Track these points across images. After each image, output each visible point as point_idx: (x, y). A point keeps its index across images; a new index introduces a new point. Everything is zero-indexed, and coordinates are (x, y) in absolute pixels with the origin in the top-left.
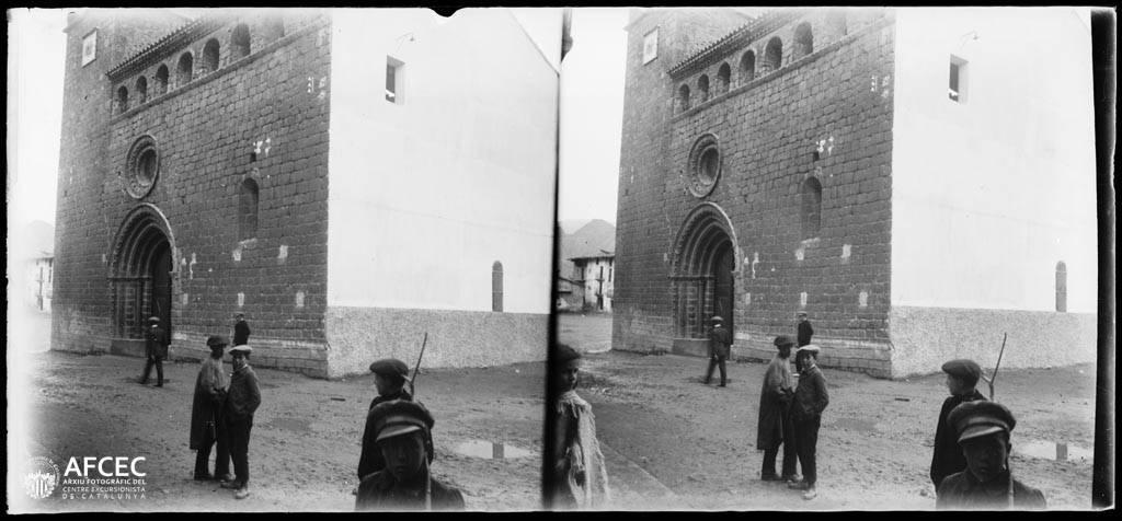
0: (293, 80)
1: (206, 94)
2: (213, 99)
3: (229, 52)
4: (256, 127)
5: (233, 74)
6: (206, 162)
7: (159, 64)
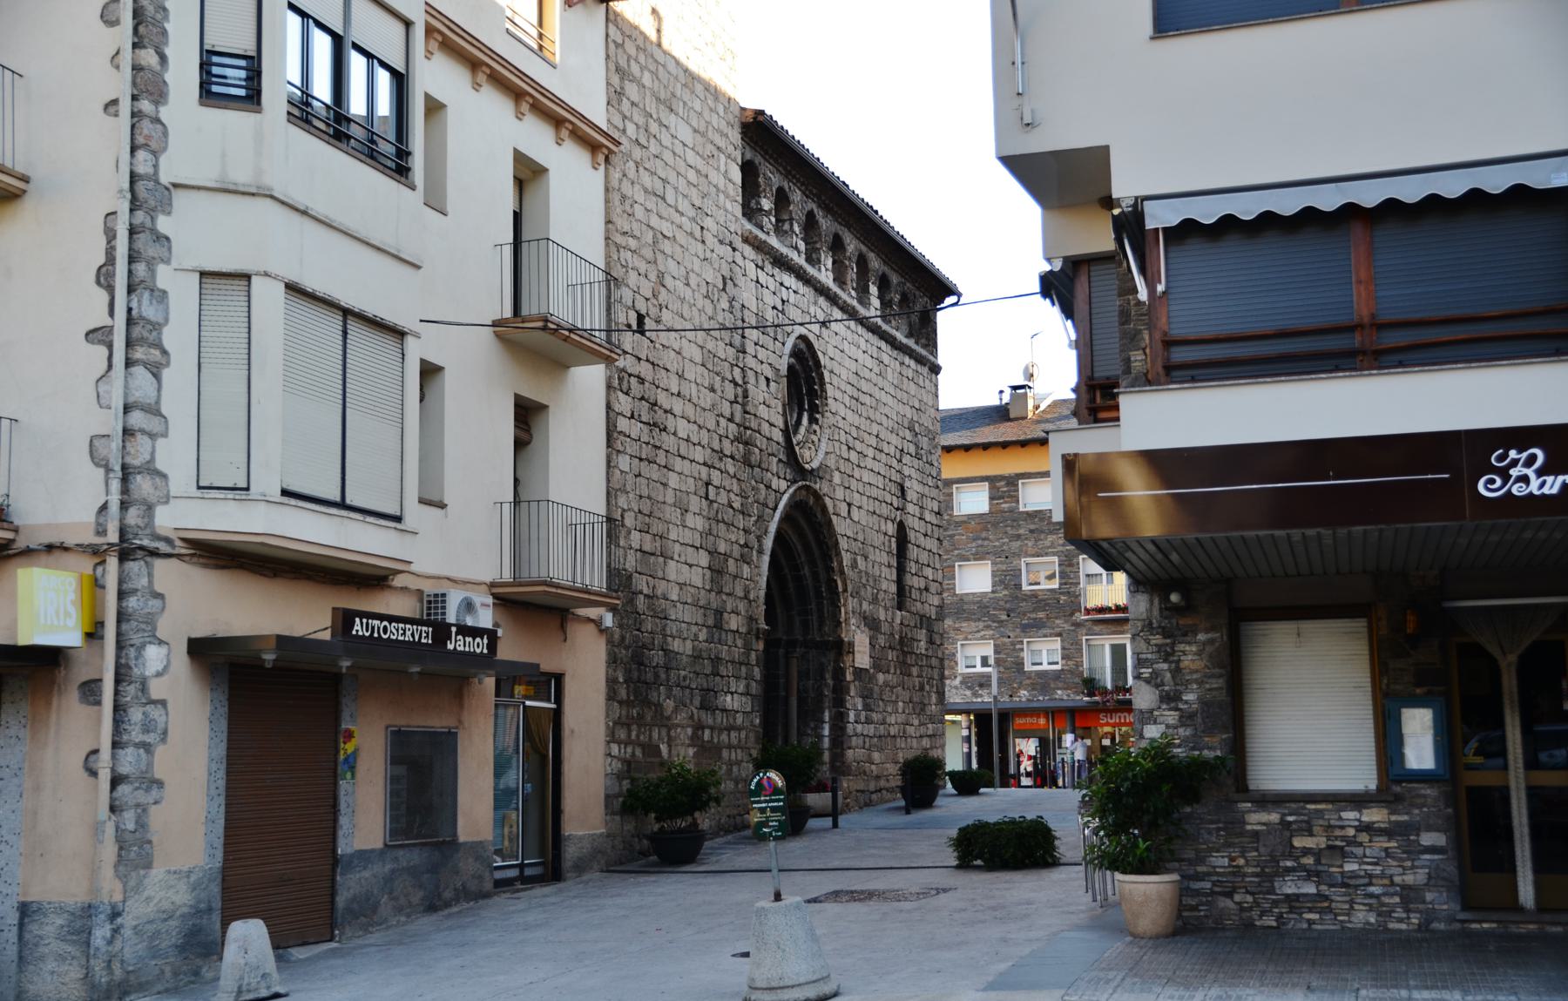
2: (853, 352)
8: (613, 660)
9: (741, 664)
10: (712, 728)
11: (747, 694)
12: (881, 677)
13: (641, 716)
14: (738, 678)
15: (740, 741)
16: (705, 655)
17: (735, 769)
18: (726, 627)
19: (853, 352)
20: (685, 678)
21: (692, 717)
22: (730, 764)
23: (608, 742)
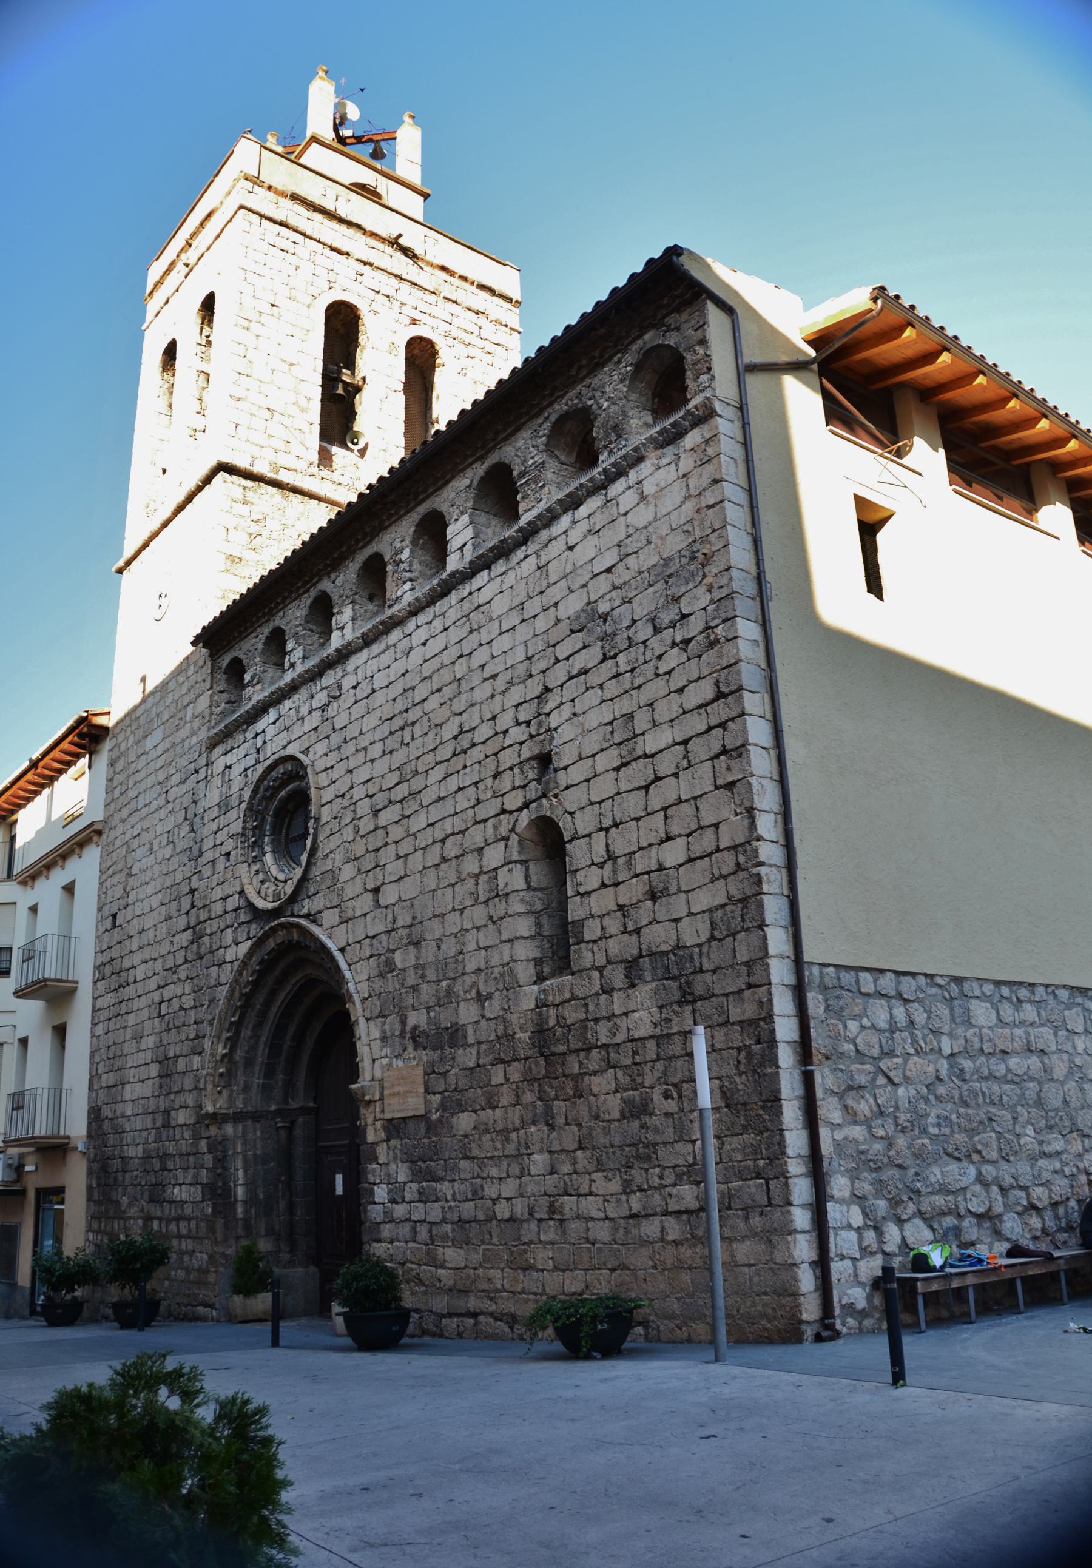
0: (631, 561)
2: (435, 646)
3: (469, 532)
4: (547, 690)
6: (427, 797)
7: (313, 593)
8: (90, 1173)
9: (189, 1154)
10: (160, 1219)
12: (464, 1122)
13: (107, 1211)
15: (190, 1231)
16: (154, 1154)
17: (186, 1258)
18: (173, 1123)
20: (137, 1177)
21: (142, 1210)
22: (181, 1253)
23: (87, 1231)
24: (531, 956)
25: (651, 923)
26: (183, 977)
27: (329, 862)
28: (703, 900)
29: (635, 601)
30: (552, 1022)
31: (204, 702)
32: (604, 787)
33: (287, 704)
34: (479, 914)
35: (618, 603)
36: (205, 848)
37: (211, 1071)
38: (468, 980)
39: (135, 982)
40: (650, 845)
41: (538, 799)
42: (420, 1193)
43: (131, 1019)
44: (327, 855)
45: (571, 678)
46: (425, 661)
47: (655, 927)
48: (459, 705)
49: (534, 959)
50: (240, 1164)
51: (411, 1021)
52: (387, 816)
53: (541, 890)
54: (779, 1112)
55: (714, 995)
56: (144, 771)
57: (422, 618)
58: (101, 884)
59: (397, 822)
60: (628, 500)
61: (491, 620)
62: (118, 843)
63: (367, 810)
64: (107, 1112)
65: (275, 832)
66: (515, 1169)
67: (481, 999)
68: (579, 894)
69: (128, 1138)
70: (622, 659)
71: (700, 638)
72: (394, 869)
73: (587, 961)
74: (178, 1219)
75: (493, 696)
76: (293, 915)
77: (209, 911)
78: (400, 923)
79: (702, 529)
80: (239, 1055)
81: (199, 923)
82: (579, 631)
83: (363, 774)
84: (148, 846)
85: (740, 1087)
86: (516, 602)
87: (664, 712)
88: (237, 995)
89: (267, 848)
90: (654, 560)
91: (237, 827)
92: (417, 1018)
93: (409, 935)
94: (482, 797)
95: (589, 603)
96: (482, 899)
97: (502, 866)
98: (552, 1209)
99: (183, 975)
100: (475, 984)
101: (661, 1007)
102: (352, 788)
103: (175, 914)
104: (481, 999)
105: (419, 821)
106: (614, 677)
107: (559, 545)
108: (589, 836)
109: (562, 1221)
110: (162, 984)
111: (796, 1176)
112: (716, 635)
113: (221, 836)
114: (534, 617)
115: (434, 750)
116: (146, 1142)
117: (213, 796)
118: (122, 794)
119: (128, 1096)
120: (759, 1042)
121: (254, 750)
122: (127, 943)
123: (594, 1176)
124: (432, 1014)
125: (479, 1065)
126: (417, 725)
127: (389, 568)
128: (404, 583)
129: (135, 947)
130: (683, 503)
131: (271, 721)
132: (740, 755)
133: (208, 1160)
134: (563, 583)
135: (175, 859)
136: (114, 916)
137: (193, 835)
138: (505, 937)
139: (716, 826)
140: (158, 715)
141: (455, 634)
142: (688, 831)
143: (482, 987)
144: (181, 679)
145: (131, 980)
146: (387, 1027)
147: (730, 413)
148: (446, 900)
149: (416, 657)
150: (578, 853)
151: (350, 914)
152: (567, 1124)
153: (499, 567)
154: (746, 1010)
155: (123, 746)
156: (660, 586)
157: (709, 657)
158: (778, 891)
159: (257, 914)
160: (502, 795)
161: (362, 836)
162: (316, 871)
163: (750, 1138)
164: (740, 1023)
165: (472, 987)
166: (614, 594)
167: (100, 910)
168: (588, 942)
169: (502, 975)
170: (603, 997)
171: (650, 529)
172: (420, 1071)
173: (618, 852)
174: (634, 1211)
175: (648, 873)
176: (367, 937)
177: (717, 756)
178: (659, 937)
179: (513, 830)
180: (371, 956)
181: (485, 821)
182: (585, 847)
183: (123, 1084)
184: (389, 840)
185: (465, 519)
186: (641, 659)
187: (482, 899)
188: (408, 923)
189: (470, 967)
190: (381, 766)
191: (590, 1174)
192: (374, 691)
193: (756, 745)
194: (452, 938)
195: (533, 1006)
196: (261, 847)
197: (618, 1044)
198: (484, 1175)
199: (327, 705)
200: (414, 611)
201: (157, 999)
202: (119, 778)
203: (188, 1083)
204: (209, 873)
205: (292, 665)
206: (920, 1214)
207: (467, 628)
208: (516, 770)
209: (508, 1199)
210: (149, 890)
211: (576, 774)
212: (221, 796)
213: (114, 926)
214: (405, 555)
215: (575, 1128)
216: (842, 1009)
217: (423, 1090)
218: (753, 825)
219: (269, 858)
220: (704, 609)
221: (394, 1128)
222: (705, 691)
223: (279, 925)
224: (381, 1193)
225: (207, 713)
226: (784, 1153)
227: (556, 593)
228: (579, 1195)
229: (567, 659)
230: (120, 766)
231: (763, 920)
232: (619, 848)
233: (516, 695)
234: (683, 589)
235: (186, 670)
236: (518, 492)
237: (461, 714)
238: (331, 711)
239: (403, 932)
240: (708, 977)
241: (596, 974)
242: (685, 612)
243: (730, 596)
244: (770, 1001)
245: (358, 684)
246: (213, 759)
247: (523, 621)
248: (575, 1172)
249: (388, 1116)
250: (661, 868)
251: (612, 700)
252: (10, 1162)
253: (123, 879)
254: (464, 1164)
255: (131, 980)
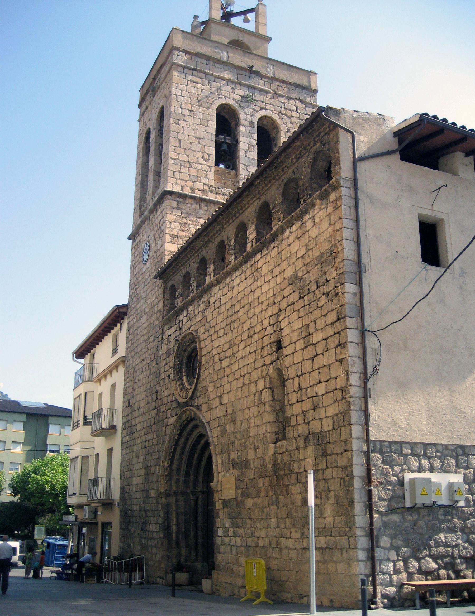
0: (310, 253)
1: (237, 281)
2: (243, 286)
3: (254, 234)
4: (280, 310)
5: (258, 256)
6: (239, 355)
9: (155, 510)
10: (145, 539)
11: (157, 523)
12: (249, 502)
14: (154, 517)
17: (154, 556)
19: (243, 286)
21: (139, 534)
23: (120, 542)
24: (274, 430)
25: (313, 420)
26: (153, 431)
27: (205, 382)
28: (332, 411)
29: (311, 272)
30: (279, 461)
31: (161, 305)
32: (298, 357)
33: (190, 308)
34: (255, 410)
35: (305, 272)
36: (161, 373)
37: (163, 474)
38: (252, 439)
39: (137, 431)
40: (314, 385)
41: (277, 360)
42: (234, 533)
43: (135, 448)
44: (204, 379)
45: (288, 306)
46: (239, 293)
47: (314, 422)
48: (250, 315)
49: (275, 432)
50: (174, 515)
51: (232, 457)
52: (225, 363)
53: (278, 401)
54: (353, 508)
55: (333, 454)
56: (140, 334)
57: (238, 273)
58: (124, 385)
59: (228, 366)
60: (309, 224)
61: (261, 276)
62: (131, 367)
63: (218, 360)
64: (126, 490)
65: (188, 366)
66: (266, 525)
67: (256, 448)
68: (289, 404)
69: (134, 501)
70: (306, 298)
71: (333, 292)
72: (227, 387)
73: (291, 435)
74: (151, 539)
75: (262, 311)
76: (192, 406)
77: (162, 401)
78: (228, 412)
79: (335, 241)
80: (175, 466)
81: (159, 406)
82: (292, 284)
83: (216, 344)
84: (141, 369)
85: (341, 495)
86: (270, 269)
87: (321, 324)
88: (172, 440)
89: (184, 374)
90: (318, 254)
91: (172, 364)
92: (233, 455)
93: (232, 418)
94: (257, 358)
95: (296, 271)
96: (256, 404)
97: (263, 390)
98: (278, 543)
99: (153, 429)
100: (253, 442)
101: (316, 458)
102: (213, 349)
103: (150, 401)
104: (256, 448)
105: (236, 367)
106: (303, 307)
107: (284, 244)
108: (293, 378)
109: (281, 549)
110: (146, 433)
111: (360, 536)
112: (338, 290)
113: (167, 367)
114: (276, 276)
115: (241, 335)
116: (140, 504)
117: (164, 349)
118: (132, 344)
119: (134, 483)
120: (348, 476)
121: (178, 329)
122: (134, 413)
123: (292, 530)
124: (239, 454)
125: (254, 478)
126: (236, 322)
127: (227, 247)
128: (232, 255)
129: (136, 416)
130: (328, 228)
131: (185, 315)
132: (345, 347)
133: (162, 513)
134: (286, 262)
135: (151, 376)
136: (129, 401)
137: (157, 366)
138: (264, 422)
139: (336, 378)
140: (145, 309)
141: (249, 281)
142: (326, 380)
143: (256, 443)
144: (153, 293)
145: (135, 431)
146: (224, 458)
147: (349, 184)
148: (244, 403)
149: (236, 291)
150: (292, 385)
151: (211, 406)
152: (283, 506)
153: (265, 252)
154: (342, 462)
155: (132, 322)
156: (319, 266)
157: (336, 300)
158: (359, 408)
159: (179, 404)
160: (264, 357)
161: (216, 372)
162: (200, 386)
163: (343, 518)
164: (341, 467)
165: (252, 443)
166: (304, 268)
167: (124, 397)
168: (292, 426)
169: (263, 438)
170: (296, 451)
171: (317, 239)
172: (234, 479)
173: (303, 387)
174: (305, 546)
175: (313, 397)
176: (217, 417)
177: (337, 347)
178: (315, 426)
179: (267, 374)
180: (219, 426)
181: (257, 369)
182: (292, 383)
183: (132, 477)
184: (225, 374)
185: (253, 227)
186: (312, 300)
187: (256, 404)
188: (232, 412)
189: (252, 434)
190: (223, 340)
191: (290, 529)
192: (221, 305)
193: (351, 342)
194: (246, 421)
195: (273, 453)
196: (181, 373)
197: (301, 472)
198: (255, 526)
199: (205, 310)
200: (235, 269)
201: (144, 440)
202: (131, 337)
203: (155, 479)
204: (162, 384)
205: (193, 290)
206: (430, 556)
207: (253, 279)
208: (269, 346)
209: (263, 538)
210: (142, 390)
211: (288, 351)
212: (167, 349)
213: (129, 405)
214: (232, 242)
215: (285, 508)
216: (391, 461)
217: (234, 487)
218: (348, 379)
219: (184, 378)
220: (334, 278)
221: (226, 503)
222: (332, 317)
223: (186, 409)
224: (220, 532)
225: (162, 310)
226: (354, 525)
227: (284, 265)
228: (286, 538)
229: (287, 297)
230: (131, 331)
231: (350, 422)
232: (303, 386)
233: (269, 313)
234: (328, 268)
235: (155, 288)
236: (272, 216)
237: (251, 318)
238: (206, 313)
239: (229, 416)
240: (331, 445)
241: (294, 441)
242: (328, 279)
243: (343, 273)
244: (352, 458)
245: (215, 301)
246: (164, 331)
247: (273, 277)
248: (286, 528)
249: (223, 498)
250: (317, 396)
251: (302, 317)
252: (92, 510)
253: (132, 384)
254: (248, 521)
255: (135, 431)
